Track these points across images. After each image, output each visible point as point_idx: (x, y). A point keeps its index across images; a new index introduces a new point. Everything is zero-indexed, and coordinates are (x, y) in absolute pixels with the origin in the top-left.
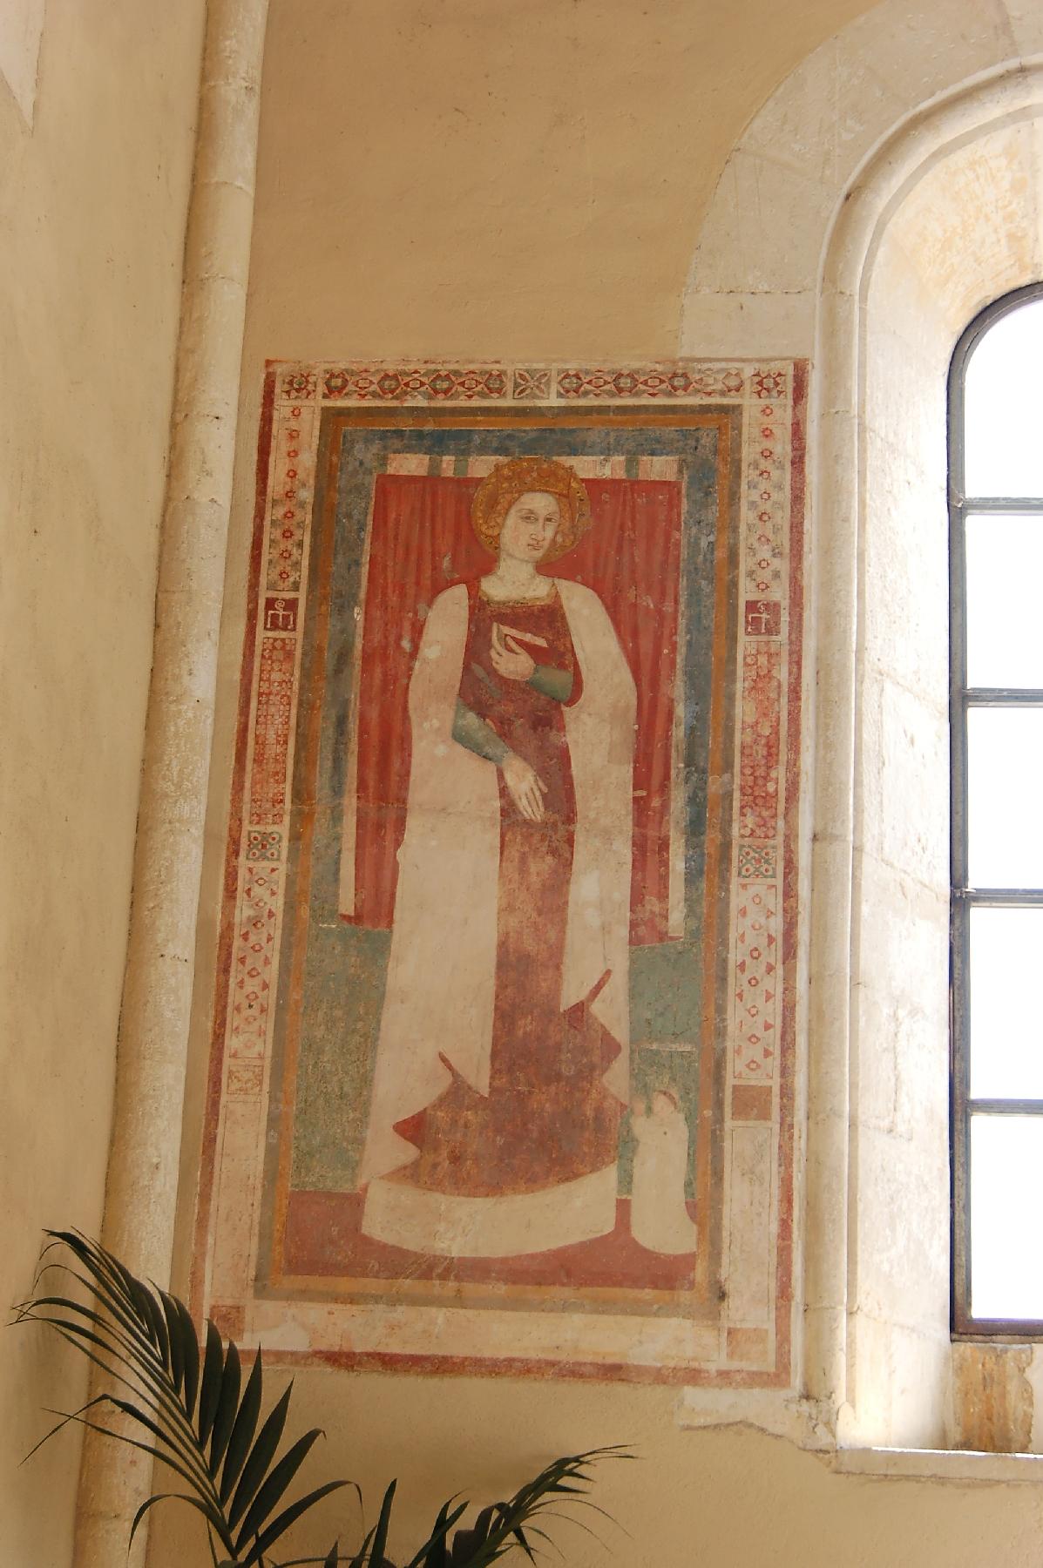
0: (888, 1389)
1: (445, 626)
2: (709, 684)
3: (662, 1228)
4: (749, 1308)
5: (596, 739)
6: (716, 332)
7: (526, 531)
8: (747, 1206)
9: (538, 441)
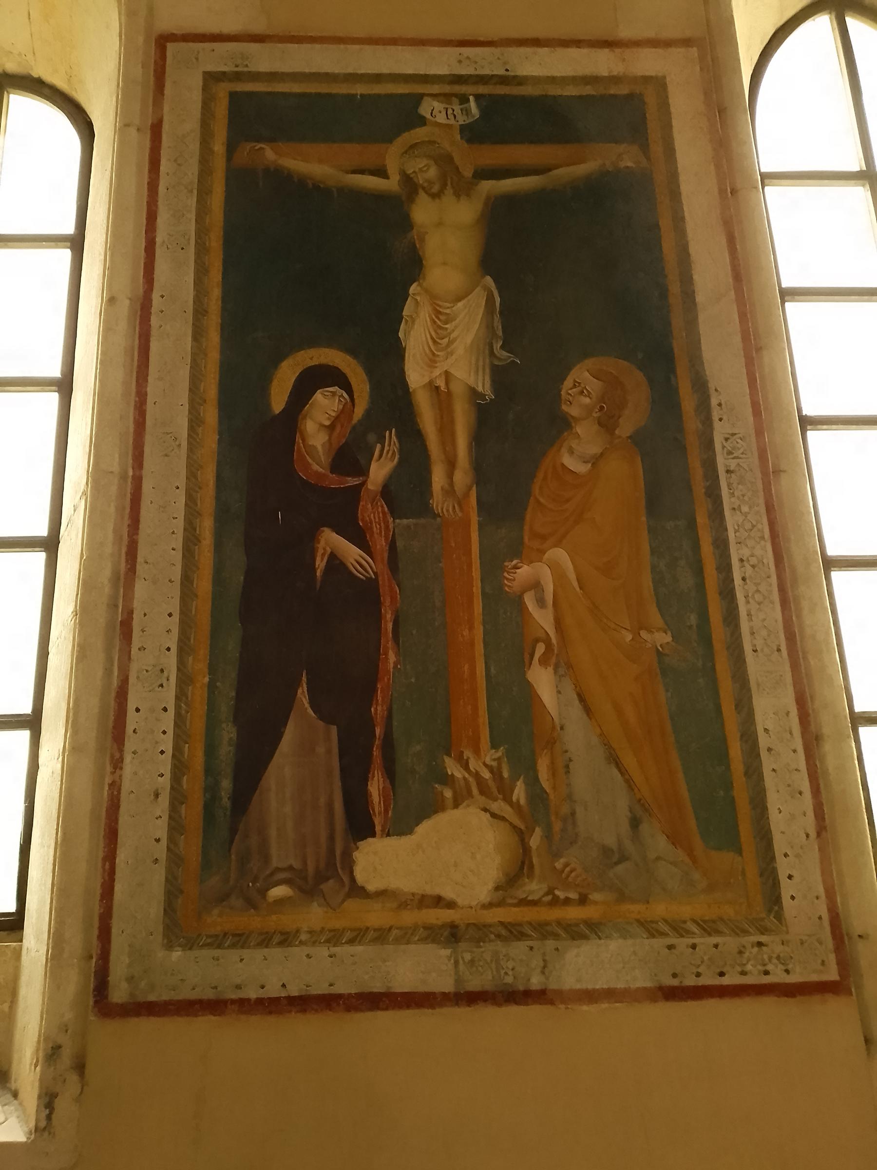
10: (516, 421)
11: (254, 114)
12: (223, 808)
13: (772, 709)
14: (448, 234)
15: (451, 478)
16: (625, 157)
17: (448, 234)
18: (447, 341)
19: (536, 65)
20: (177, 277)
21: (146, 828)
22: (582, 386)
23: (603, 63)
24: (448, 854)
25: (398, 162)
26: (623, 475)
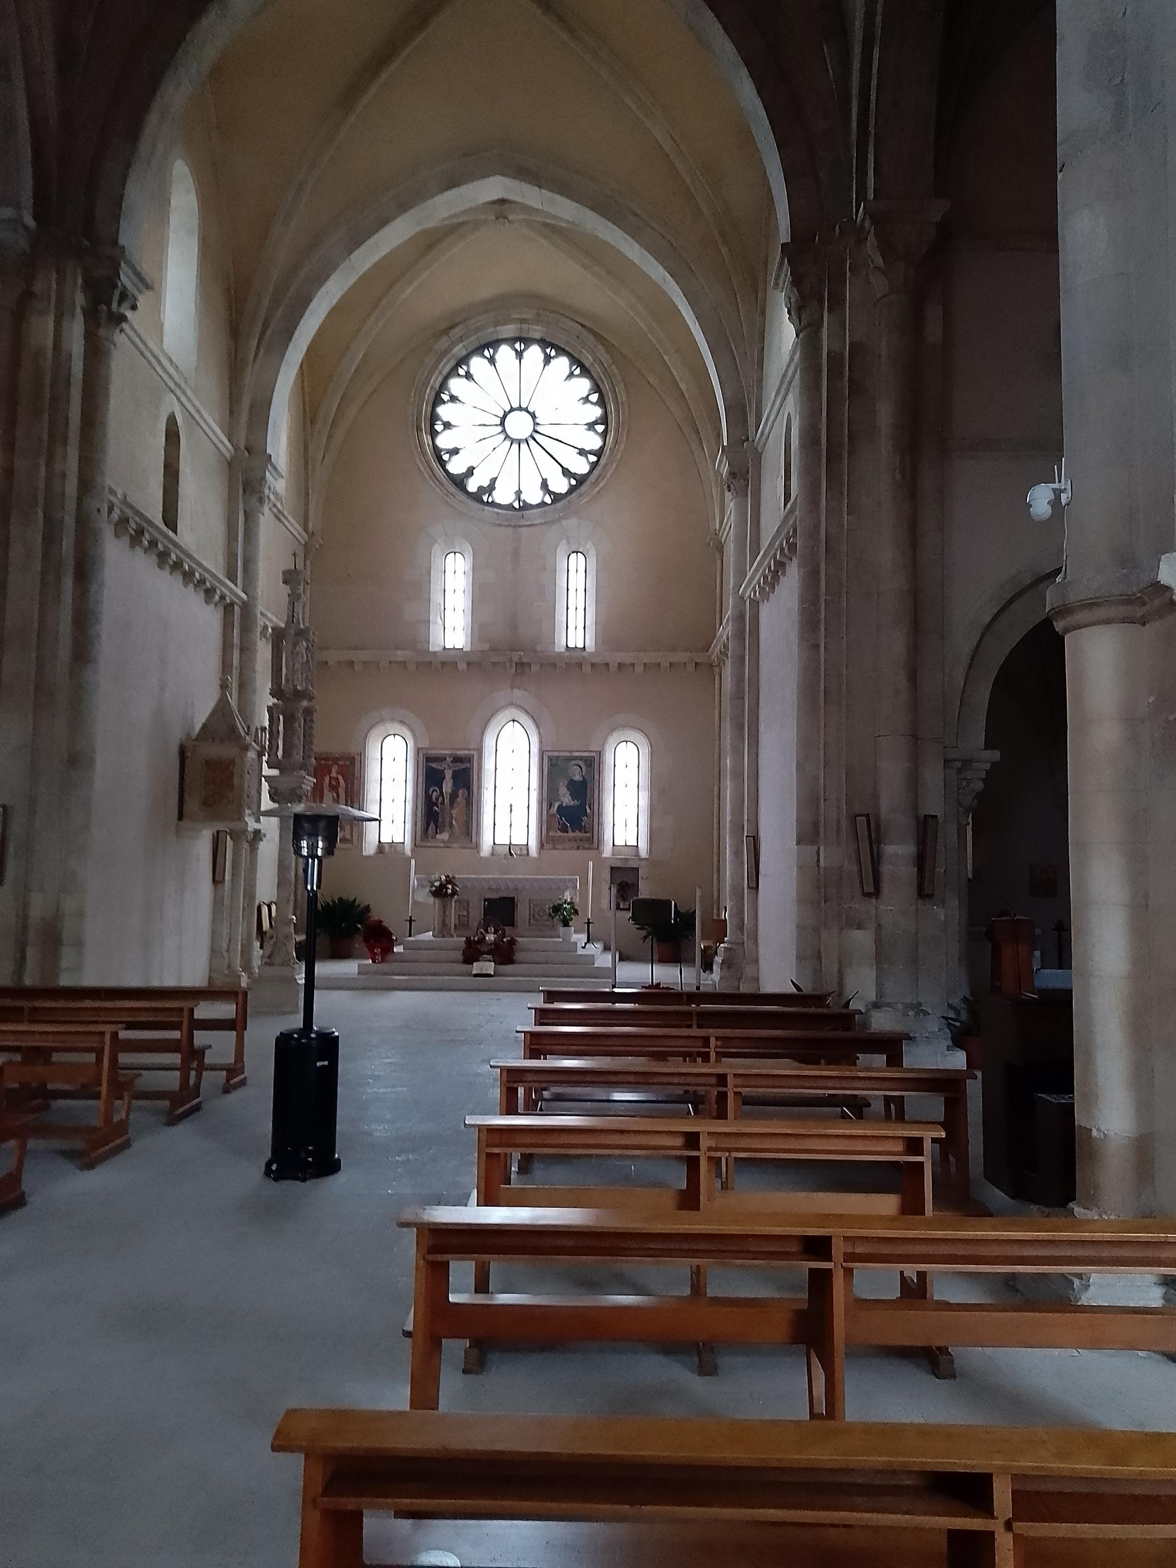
0: (370, 848)
1: (327, 779)
2: (353, 786)
3: (348, 837)
4: (355, 842)
5: (341, 791)
6: (353, 750)
7: (334, 769)
8: (355, 835)
9: (337, 759)
10: (454, 796)
11: (428, 759)
12: (425, 831)
13: (474, 825)
14: (448, 774)
15: (447, 801)
16: (467, 765)
17: (448, 774)
18: (447, 786)
19: (460, 753)
20: (420, 779)
21: (419, 832)
22: (460, 792)
23: (467, 752)
24: (444, 836)
25: (444, 765)
26: (464, 802)
